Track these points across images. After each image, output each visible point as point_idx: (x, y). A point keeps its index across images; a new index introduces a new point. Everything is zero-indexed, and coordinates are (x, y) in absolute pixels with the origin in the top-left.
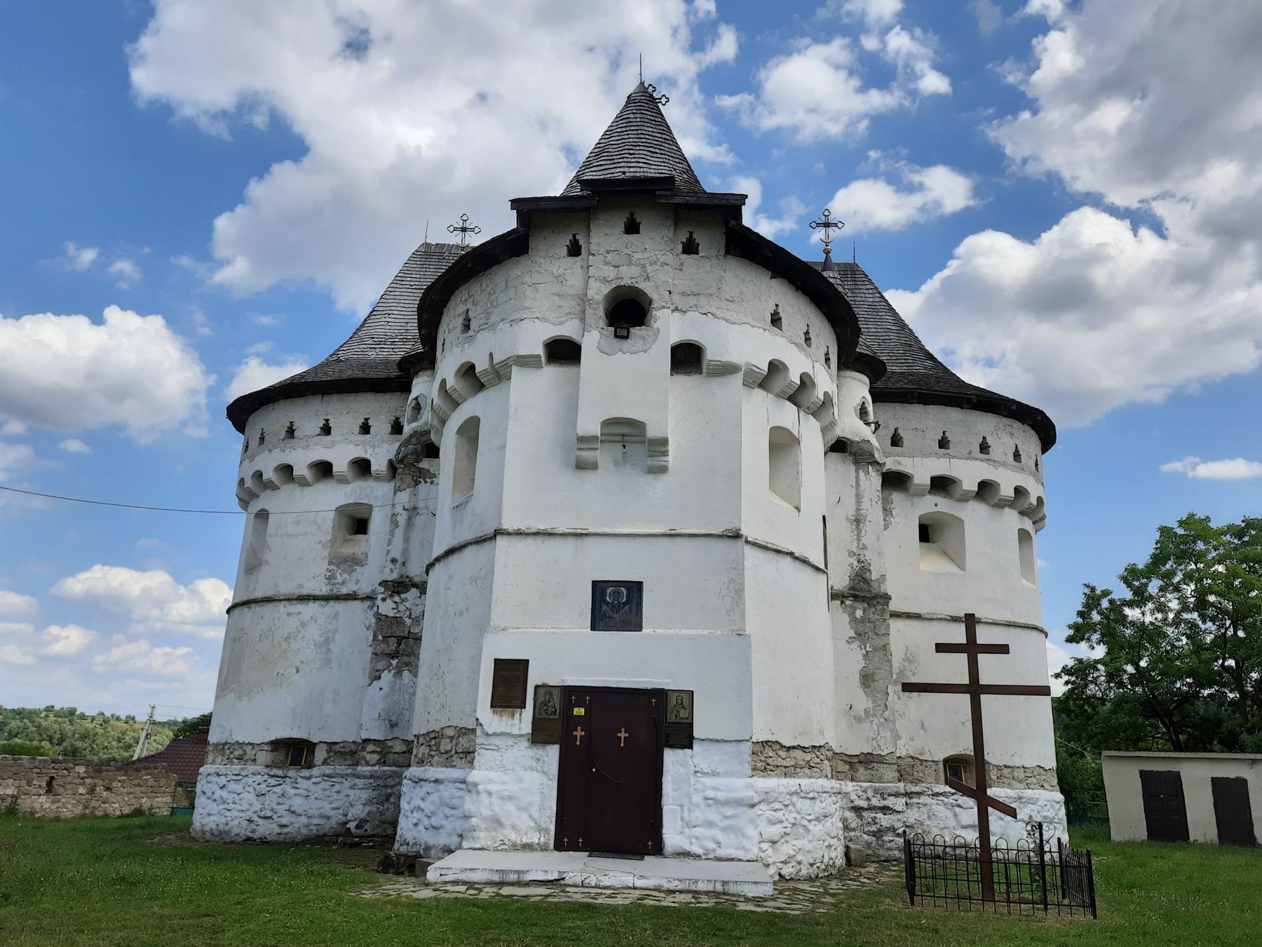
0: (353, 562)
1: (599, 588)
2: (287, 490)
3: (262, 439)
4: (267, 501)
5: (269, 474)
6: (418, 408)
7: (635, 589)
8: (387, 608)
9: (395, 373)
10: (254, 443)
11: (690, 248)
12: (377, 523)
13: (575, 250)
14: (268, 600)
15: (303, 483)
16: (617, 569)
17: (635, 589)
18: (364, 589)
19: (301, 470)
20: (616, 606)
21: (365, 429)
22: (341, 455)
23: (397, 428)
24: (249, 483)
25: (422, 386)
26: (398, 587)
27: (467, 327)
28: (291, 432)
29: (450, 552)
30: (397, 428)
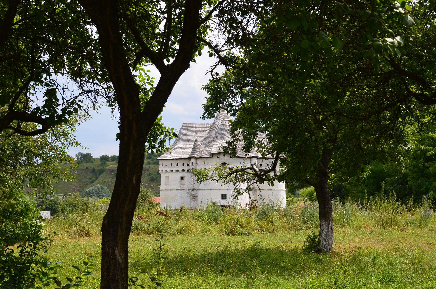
0: (183, 184)
1: (222, 195)
2: (172, 173)
3: (166, 165)
4: (167, 174)
5: (169, 171)
6: (193, 164)
7: (226, 195)
8: (192, 193)
9: (187, 157)
10: (164, 165)
11: (231, 157)
12: (186, 179)
13: (218, 157)
14: (171, 190)
15: (174, 173)
16: (224, 193)
17: (226, 195)
18: (186, 189)
19: (174, 171)
20: (224, 197)
21: (183, 165)
22: (180, 169)
23: (188, 165)
24: (164, 171)
25: (193, 161)
26: (193, 190)
27: (205, 163)
28: (172, 165)
29: (205, 190)
30: (188, 165)
